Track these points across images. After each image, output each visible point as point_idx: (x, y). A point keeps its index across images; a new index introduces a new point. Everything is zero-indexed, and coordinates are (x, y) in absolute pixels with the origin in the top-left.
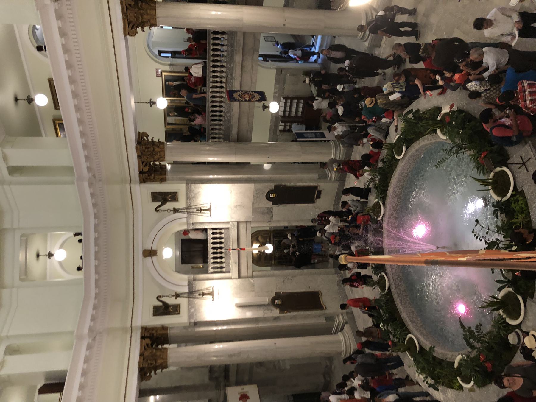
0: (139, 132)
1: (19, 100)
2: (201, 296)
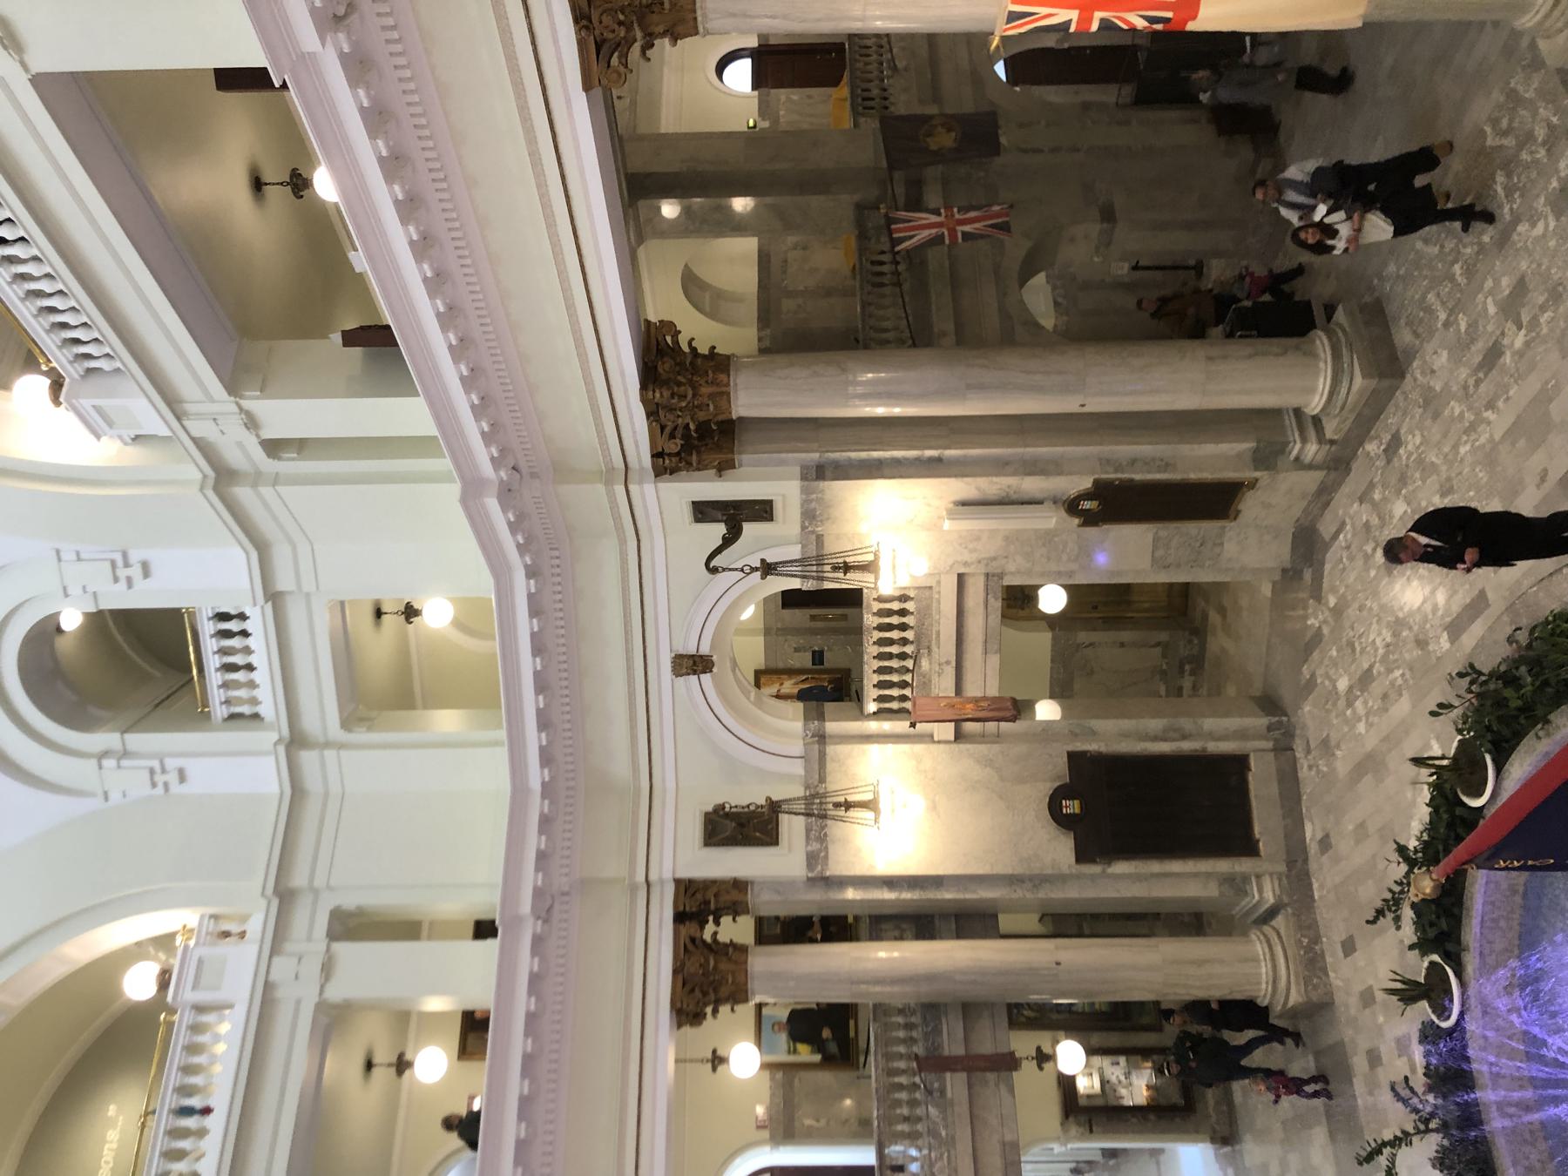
0: (648, 322)
1: (266, 184)
2: (841, 812)
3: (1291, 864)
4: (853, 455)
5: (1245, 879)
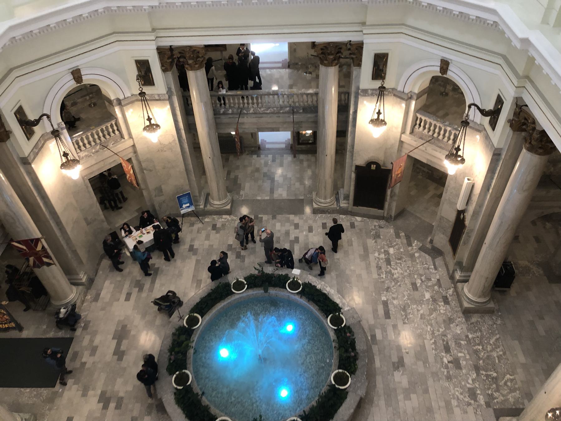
3: (351, 212)
4: (499, 168)
5: (348, 200)
